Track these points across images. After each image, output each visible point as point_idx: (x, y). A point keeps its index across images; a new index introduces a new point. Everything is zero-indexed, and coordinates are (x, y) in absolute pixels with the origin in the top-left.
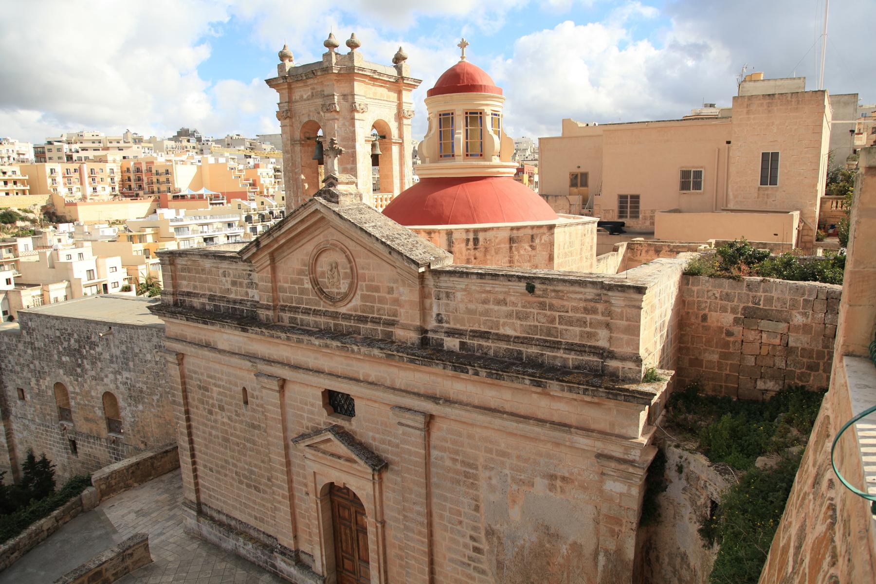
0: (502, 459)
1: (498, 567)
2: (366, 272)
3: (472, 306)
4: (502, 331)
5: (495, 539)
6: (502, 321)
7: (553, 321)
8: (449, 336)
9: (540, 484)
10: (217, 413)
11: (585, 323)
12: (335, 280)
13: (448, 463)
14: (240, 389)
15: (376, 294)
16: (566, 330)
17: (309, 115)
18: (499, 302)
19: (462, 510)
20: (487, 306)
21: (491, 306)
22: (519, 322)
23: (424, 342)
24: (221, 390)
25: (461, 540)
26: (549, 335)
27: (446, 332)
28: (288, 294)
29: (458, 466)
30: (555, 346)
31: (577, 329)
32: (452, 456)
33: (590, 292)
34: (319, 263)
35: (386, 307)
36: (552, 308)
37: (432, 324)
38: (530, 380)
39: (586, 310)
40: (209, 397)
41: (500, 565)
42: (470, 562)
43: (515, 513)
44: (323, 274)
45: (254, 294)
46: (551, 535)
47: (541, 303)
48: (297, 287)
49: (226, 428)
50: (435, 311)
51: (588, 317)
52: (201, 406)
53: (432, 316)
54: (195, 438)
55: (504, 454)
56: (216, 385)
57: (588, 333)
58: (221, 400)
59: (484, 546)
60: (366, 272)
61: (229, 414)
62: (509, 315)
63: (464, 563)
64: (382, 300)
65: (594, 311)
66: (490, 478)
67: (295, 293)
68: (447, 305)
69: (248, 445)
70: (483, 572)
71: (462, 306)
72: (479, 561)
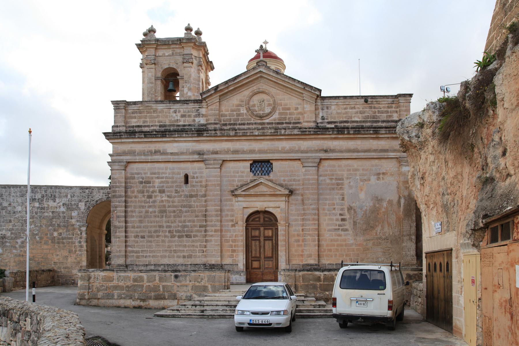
0: (355, 172)
1: (354, 225)
2: (283, 102)
3: (339, 111)
4: (353, 119)
5: (352, 211)
6: (353, 115)
7: (375, 112)
8: (329, 124)
9: (373, 179)
10: (156, 196)
11: (388, 112)
12: (263, 107)
13: (328, 181)
14: (182, 176)
15: (288, 111)
16: (381, 116)
17: (169, 65)
18: (352, 108)
19: (335, 202)
20: (346, 110)
21: (348, 110)
22: (361, 115)
23: (317, 127)
24: (164, 180)
25: (335, 218)
26: (374, 118)
27: (327, 123)
28: (228, 117)
29: (334, 181)
30: (378, 122)
31: (385, 115)
32: (330, 177)
33: (390, 100)
34: (251, 100)
35: (293, 116)
36: (375, 108)
37: (319, 121)
38: (373, 131)
39: (388, 107)
40: (149, 187)
41: (355, 223)
42: (339, 228)
43: (362, 195)
44: (254, 106)
45: (203, 121)
46: (378, 200)
47: (370, 107)
48: (235, 113)
49: (164, 204)
50: (321, 115)
51: (389, 110)
52: (140, 195)
53: (319, 118)
54: (129, 219)
55: (356, 170)
56: (158, 178)
57: (389, 115)
58: (163, 186)
59: (347, 216)
60: (283, 102)
61: (168, 194)
62: (357, 113)
63: (336, 229)
64: (291, 114)
65: (391, 107)
66: (350, 183)
67: (234, 116)
68: (327, 112)
69: (184, 209)
70: (347, 230)
71: (334, 112)
72: (344, 225)
